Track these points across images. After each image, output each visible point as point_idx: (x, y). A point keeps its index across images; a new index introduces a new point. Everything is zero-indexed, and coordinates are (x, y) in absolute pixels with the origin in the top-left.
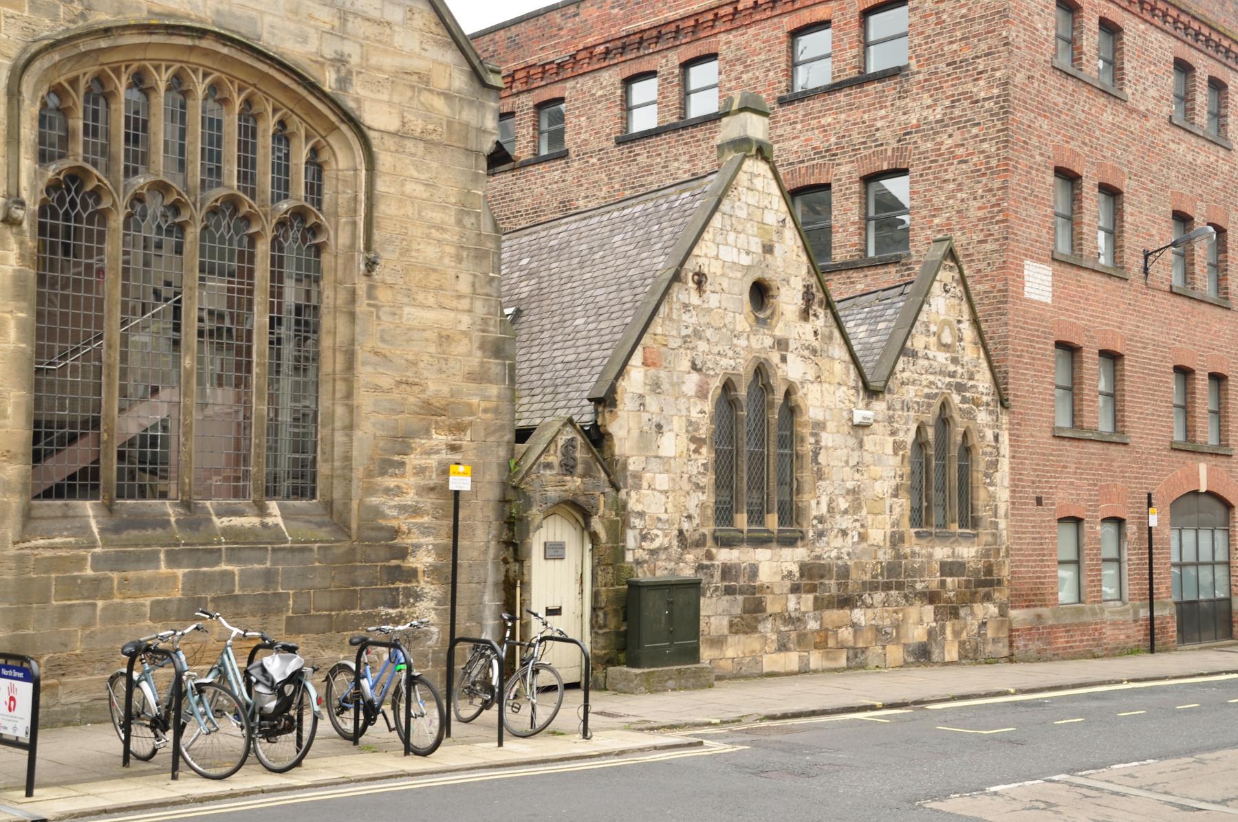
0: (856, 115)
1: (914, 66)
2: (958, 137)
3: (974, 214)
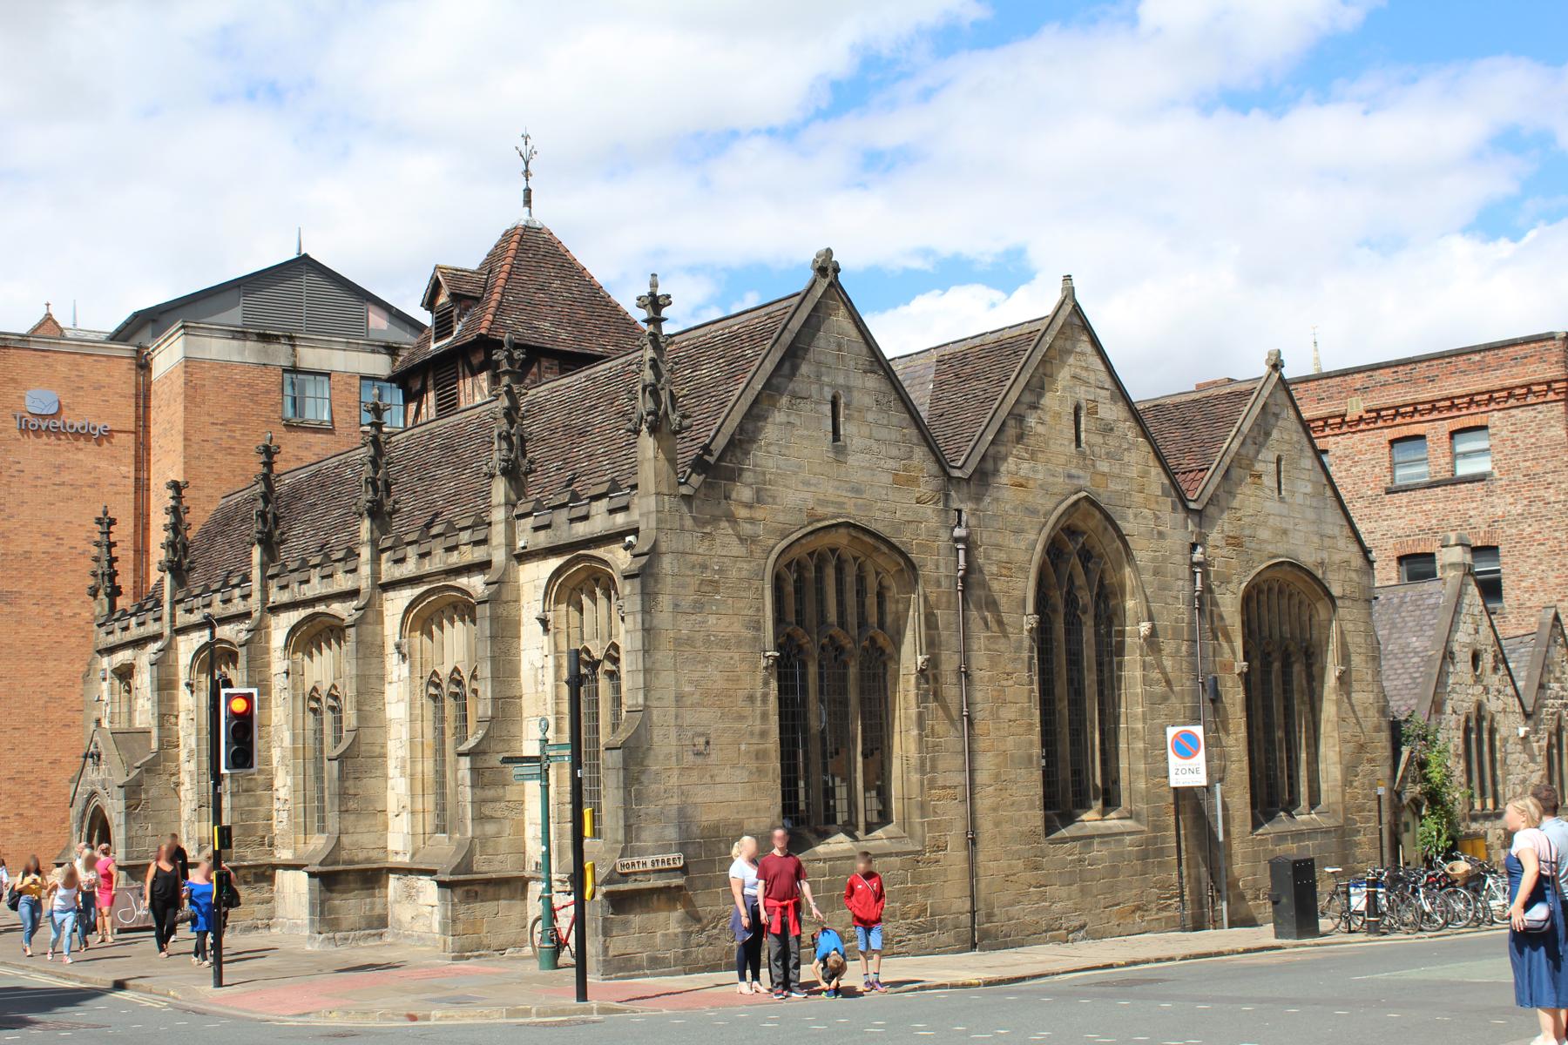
0: (1451, 506)
1: (1496, 474)
2: (1536, 527)
3: (1552, 581)
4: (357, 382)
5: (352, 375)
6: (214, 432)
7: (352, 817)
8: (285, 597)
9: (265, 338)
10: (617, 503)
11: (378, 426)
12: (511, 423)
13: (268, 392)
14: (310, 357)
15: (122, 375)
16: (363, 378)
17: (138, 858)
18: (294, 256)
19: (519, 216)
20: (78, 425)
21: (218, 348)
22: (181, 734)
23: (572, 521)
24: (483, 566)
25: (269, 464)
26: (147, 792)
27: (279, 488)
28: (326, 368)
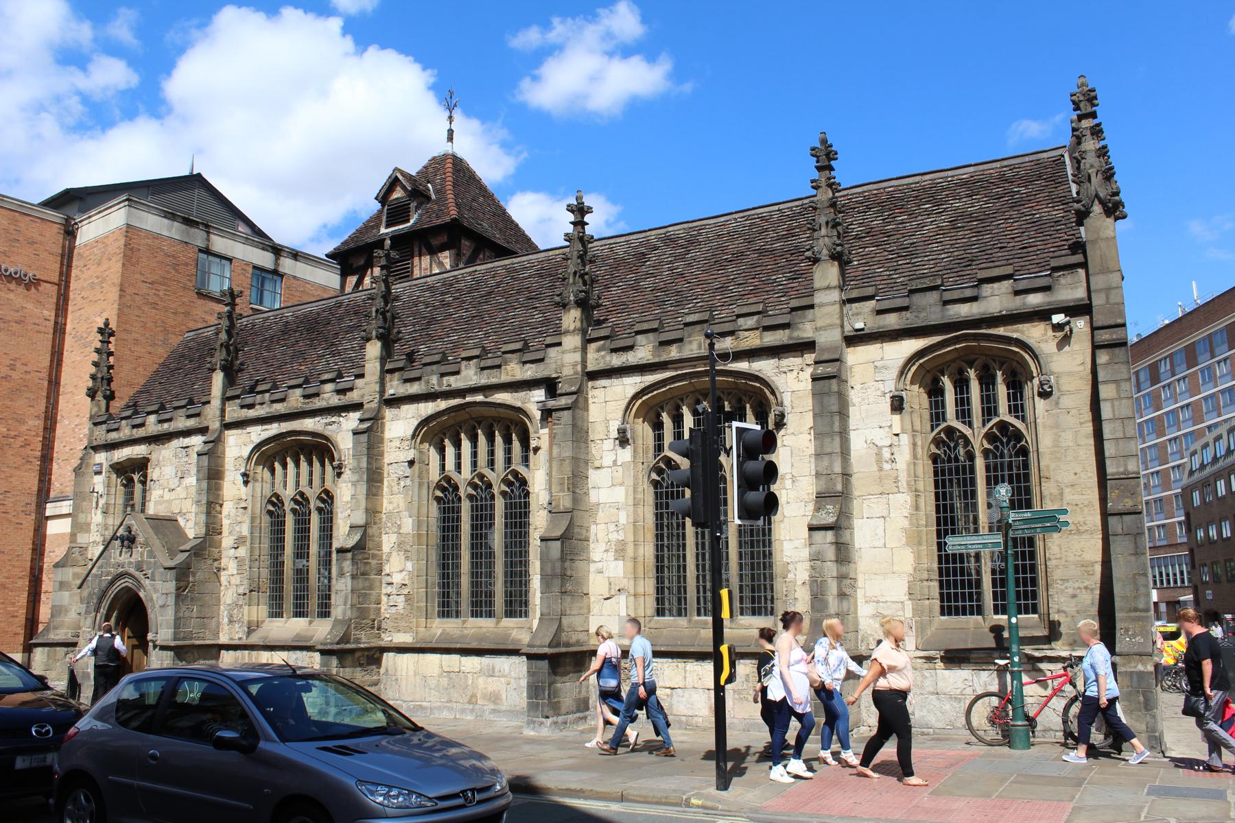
4: (250, 270)
5: (248, 264)
6: (144, 289)
7: (568, 599)
8: (414, 389)
9: (188, 222)
10: (191, 412)
11: (580, 224)
12: (386, 304)
13: (186, 264)
14: (220, 244)
15: (52, 237)
16: (255, 267)
17: (184, 639)
18: (187, 173)
19: (447, 148)
20: (12, 270)
21: (152, 222)
22: (226, 522)
23: (946, 303)
24: (203, 431)
25: (580, 224)
26: (194, 574)
27: (238, 324)
28: (230, 254)
